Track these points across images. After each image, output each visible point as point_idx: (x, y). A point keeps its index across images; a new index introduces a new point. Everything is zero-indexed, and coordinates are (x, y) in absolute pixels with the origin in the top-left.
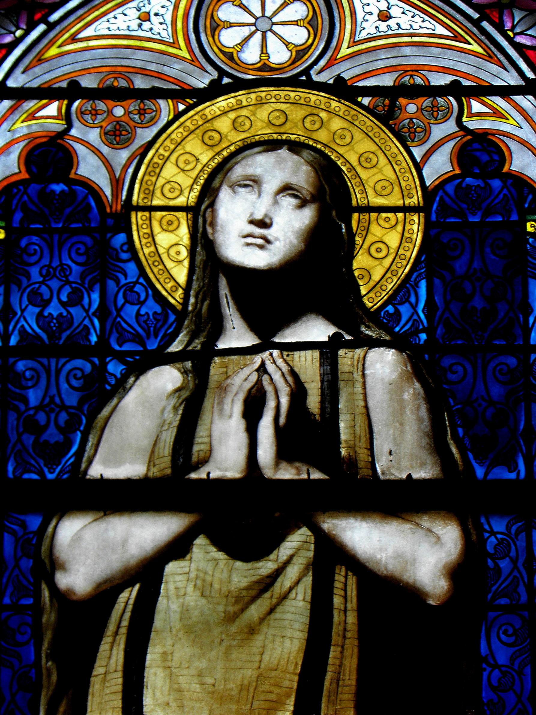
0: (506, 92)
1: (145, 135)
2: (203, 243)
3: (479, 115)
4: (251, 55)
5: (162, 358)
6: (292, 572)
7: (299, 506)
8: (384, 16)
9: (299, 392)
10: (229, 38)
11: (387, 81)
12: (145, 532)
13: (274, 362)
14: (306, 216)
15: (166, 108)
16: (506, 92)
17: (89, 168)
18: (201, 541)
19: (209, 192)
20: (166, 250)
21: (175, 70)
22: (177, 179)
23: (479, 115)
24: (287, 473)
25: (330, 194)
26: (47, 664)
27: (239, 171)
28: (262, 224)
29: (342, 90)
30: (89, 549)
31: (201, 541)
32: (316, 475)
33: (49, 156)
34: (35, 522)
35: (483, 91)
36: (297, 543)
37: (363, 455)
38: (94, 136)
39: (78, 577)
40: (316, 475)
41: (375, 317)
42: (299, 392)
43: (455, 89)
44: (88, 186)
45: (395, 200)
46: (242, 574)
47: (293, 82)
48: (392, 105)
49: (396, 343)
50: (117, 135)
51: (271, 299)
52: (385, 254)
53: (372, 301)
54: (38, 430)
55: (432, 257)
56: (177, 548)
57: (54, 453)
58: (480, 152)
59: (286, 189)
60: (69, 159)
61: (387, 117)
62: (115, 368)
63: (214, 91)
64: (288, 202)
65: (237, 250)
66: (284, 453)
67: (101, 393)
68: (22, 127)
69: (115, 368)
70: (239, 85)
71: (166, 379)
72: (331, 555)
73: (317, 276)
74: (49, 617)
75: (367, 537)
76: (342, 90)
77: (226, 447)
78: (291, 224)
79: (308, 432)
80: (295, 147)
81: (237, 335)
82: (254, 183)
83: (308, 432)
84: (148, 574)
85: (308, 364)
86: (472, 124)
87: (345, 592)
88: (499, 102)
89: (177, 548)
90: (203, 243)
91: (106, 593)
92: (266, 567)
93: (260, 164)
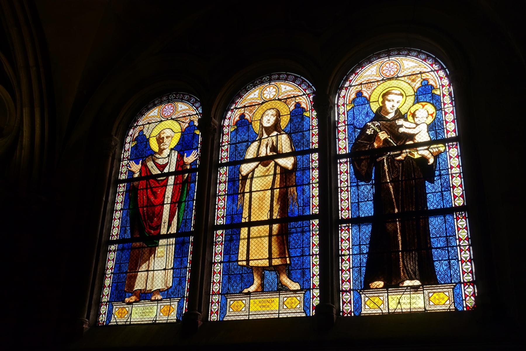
0: (301, 96)
1: (254, 111)
2: (261, 124)
3: (298, 100)
4: (268, 98)
5: (256, 141)
6: (272, 167)
7: (272, 158)
8: (285, 88)
9: (273, 143)
11: (286, 97)
12: (253, 165)
13: (270, 139)
14: (274, 118)
15: (257, 106)
16: (301, 96)
17: (247, 117)
18: (260, 165)
19: (262, 117)
20: (256, 127)
21: (258, 101)
22: (258, 116)
23: (298, 100)
24: (271, 154)
25: (278, 115)
26: (240, 185)
27: (266, 113)
28: (269, 120)
29: (279, 100)
30: (245, 169)
31: (260, 165)
32: (275, 153)
33: (242, 116)
34: (239, 166)
36: (272, 164)
37: (281, 150)
38: (248, 112)
39: (244, 173)
40: (275, 153)
41: (283, 130)
42: (273, 143)
43: (294, 97)
45: (286, 114)
46: (265, 169)
47: (274, 100)
48: (285, 101)
49: (286, 133)
50: (251, 111)
51: (269, 131)
52: (284, 122)
53: (282, 129)
54: (240, 153)
55: (291, 120)
56: (257, 167)
57: (241, 156)
58: (298, 105)
59: (272, 115)
60: (245, 116)
61: (285, 103)
62: (249, 143)
63: (263, 103)
64: (272, 117)
65: (266, 124)
66: (271, 151)
67: (248, 147)
68: (239, 113)
69: (249, 143)
70: (266, 102)
71: (256, 144)
72: (276, 164)
73: (276, 126)
74: (240, 178)
75: (282, 162)
76: (279, 100)
77: (263, 152)
78: (273, 120)
79: (274, 148)
80: (273, 109)
81: (265, 135)
82: (267, 115)
83: (274, 148)
84: (253, 171)
85: (274, 138)
86: (297, 101)
87: (278, 169)
88: (300, 97)
89: (257, 167)
90: (261, 124)
91: (247, 175)
92: (268, 167)
93: (269, 112)
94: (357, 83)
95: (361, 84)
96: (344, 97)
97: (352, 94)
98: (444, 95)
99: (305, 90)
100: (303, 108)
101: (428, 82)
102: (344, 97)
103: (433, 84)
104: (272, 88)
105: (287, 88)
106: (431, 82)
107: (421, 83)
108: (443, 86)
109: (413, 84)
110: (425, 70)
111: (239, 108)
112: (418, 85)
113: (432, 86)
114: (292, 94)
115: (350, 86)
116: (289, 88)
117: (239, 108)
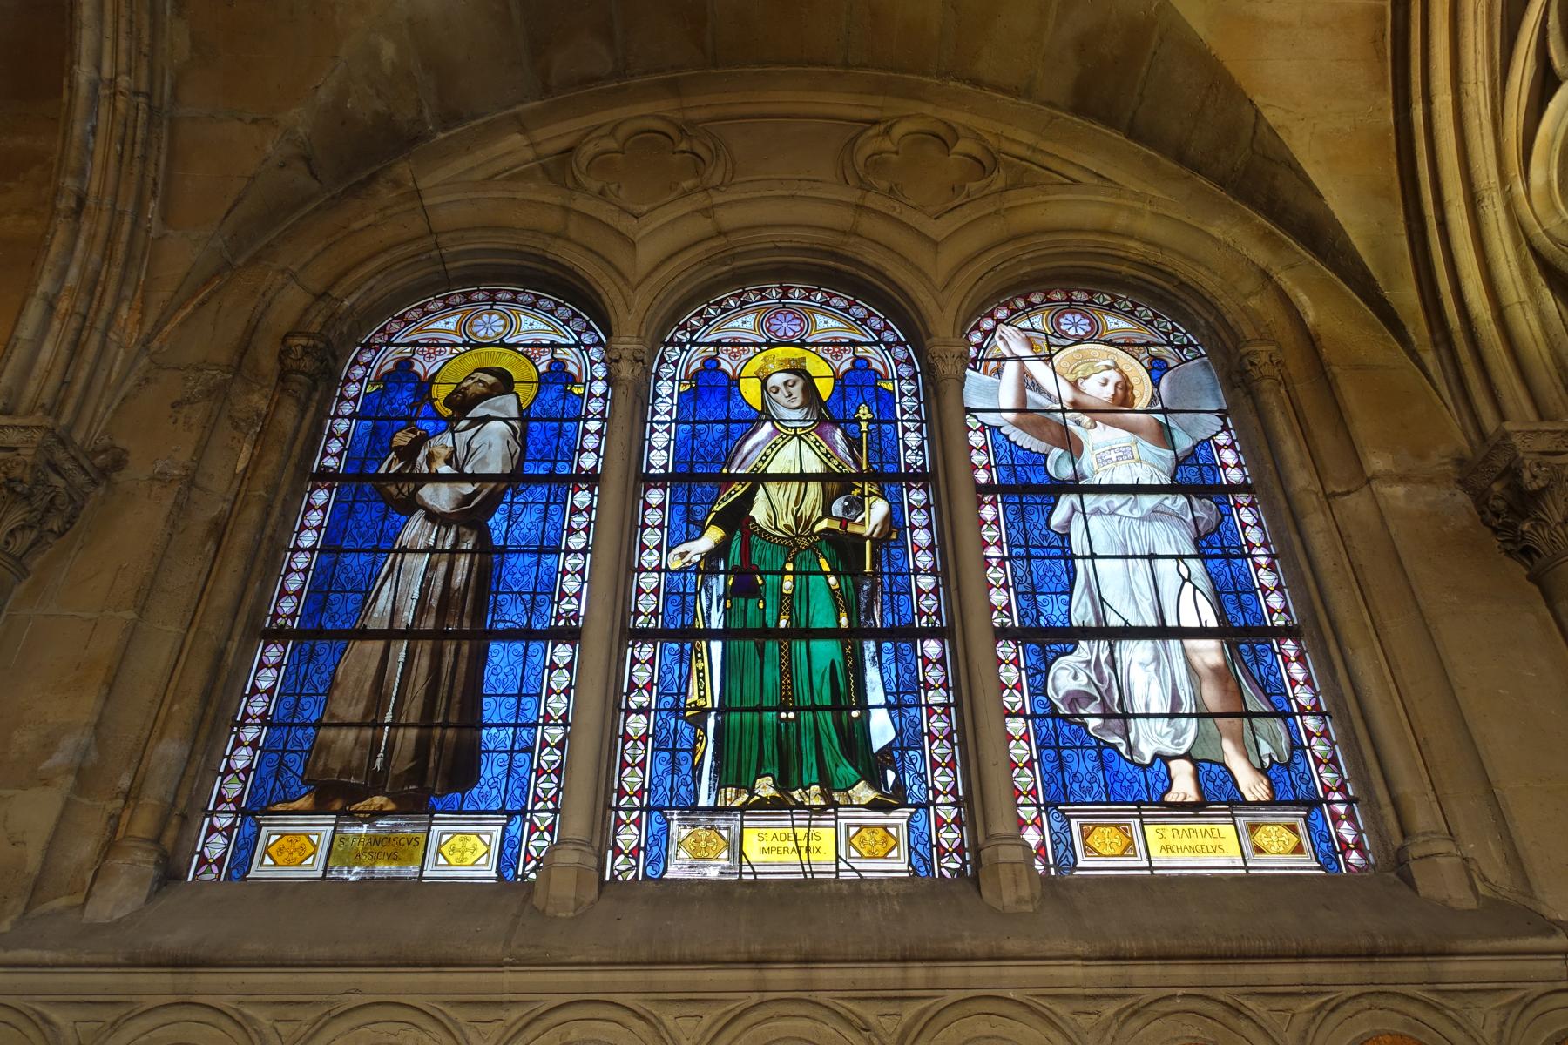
10: (475, 329)
17: (417, 368)
33: (405, 365)
35: (561, 346)
44: (417, 374)
94: (708, 340)
95: (718, 343)
96: (675, 363)
97: (695, 359)
98: (902, 395)
99: (579, 334)
100: (571, 374)
101: (869, 364)
102: (675, 363)
103: (881, 369)
104: (495, 317)
105: (532, 327)
106: (875, 365)
107: (853, 363)
108: (900, 378)
109: (837, 363)
110: (863, 339)
111: (399, 345)
112: (847, 366)
113: (877, 372)
114: (546, 338)
115: (693, 343)
116: (538, 325)
117: (399, 345)
